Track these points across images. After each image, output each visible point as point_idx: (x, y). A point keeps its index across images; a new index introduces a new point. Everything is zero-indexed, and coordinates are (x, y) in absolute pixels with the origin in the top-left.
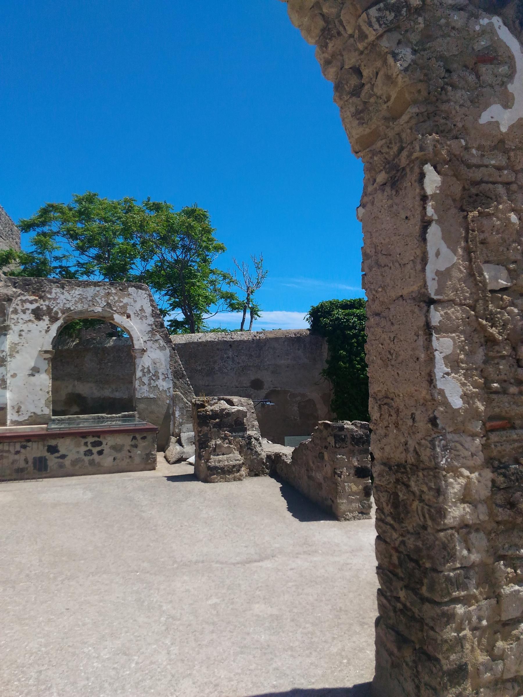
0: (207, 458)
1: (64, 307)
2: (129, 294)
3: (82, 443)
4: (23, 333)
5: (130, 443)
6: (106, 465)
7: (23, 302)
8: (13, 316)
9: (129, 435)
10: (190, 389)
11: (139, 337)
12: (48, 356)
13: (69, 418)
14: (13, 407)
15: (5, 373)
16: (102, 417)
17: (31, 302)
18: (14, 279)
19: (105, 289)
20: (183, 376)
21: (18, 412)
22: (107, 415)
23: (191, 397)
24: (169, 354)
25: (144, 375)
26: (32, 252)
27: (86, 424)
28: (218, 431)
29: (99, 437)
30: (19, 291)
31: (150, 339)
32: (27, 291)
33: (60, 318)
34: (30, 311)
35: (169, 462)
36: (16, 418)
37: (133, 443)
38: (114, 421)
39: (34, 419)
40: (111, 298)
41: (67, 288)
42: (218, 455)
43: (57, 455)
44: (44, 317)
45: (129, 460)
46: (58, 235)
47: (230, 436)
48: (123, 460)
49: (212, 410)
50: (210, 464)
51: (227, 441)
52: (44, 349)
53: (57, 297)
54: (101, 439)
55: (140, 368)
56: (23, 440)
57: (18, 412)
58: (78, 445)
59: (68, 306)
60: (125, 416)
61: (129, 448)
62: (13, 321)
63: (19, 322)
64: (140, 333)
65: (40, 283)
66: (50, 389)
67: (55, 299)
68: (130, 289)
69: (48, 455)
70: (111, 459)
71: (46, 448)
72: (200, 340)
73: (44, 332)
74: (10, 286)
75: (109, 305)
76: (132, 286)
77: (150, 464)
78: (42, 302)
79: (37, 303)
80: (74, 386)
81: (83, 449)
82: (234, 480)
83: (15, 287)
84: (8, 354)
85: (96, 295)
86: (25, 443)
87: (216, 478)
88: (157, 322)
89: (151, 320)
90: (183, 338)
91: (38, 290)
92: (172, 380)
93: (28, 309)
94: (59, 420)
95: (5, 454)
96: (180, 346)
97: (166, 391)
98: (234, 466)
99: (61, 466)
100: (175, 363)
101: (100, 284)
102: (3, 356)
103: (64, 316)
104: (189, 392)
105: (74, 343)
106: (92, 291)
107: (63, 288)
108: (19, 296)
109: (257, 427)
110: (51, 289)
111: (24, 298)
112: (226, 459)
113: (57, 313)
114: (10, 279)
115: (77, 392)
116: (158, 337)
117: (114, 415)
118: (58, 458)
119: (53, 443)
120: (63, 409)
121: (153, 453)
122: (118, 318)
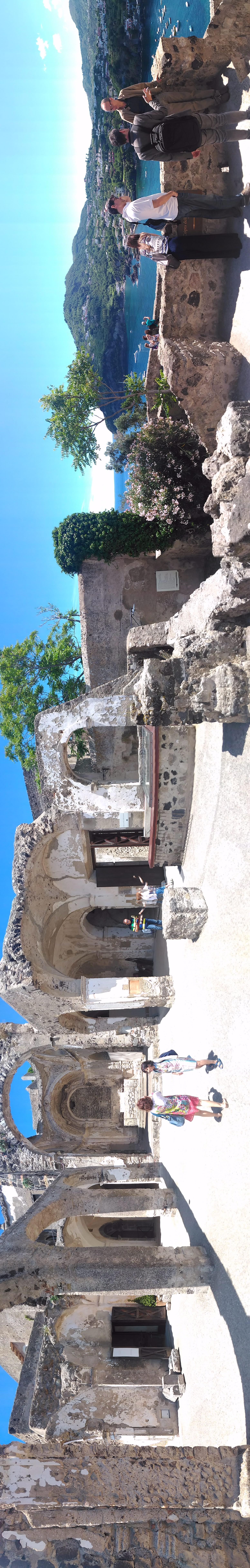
17: (60, 797)
30: (53, 805)
40: (48, 744)
41: (46, 776)
62: (73, 808)
65: (45, 792)
67: (55, 783)
75: (54, 747)
78: (58, 791)
85: (48, 756)
91: (50, 793)
93: (64, 799)
107: (46, 778)
109: (157, 625)
110: (48, 786)
111: (57, 802)
113: (64, 782)
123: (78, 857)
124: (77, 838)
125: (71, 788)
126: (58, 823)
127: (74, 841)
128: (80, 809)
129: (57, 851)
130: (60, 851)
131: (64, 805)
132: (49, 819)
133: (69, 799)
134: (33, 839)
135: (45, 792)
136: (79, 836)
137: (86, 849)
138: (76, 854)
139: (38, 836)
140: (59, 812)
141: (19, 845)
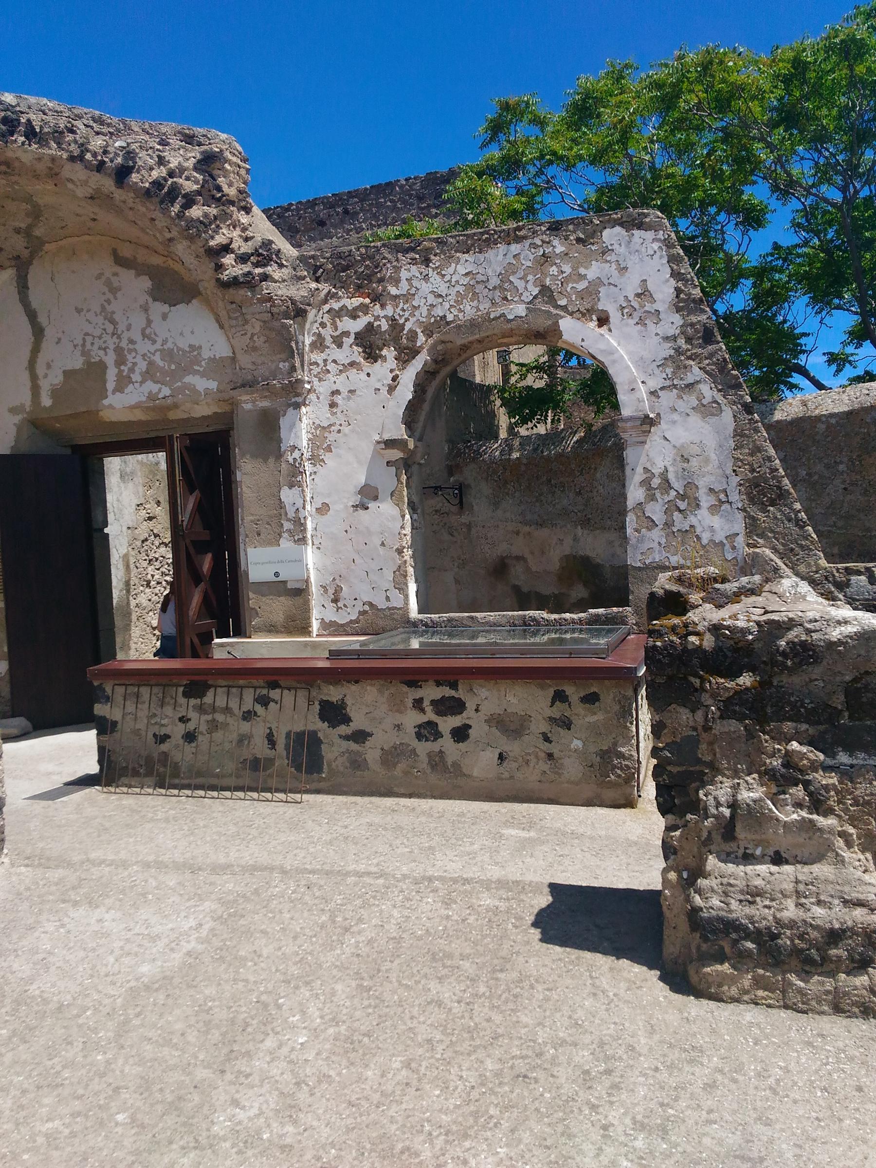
0: (691, 862)
1: (429, 315)
2: (605, 251)
3: (409, 702)
4: (338, 399)
6: (475, 774)
10: (807, 537)
13: (450, 620)
16: (534, 619)
17: (354, 317)
18: (313, 257)
19: (535, 246)
20: (781, 496)
23: (809, 565)
24: (731, 426)
25: (652, 498)
27: (493, 638)
28: (750, 735)
30: (325, 288)
31: (668, 383)
32: (344, 285)
33: (421, 347)
34: (351, 339)
36: (331, 615)
37: (557, 711)
38: (566, 632)
40: (554, 270)
41: (436, 261)
42: (747, 858)
44: (384, 352)
45: (544, 766)
46: (548, 193)
47: (815, 766)
48: (527, 762)
49: (716, 629)
50: (698, 900)
51: (798, 792)
52: (386, 436)
53: (413, 291)
54: (461, 693)
56: (261, 682)
59: (439, 312)
62: (316, 370)
63: (328, 371)
64: (637, 366)
65: (371, 258)
67: (408, 297)
68: (606, 233)
70: (491, 756)
71: (317, 707)
73: (384, 391)
74: (304, 278)
75: (546, 292)
77: (612, 785)
78: (377, 309)
79: (366, 314)
80: (576, 539)
82: (838, 1009)
83: (317, 280)
84: (307, 455)
85: (511, 269)
87: (733, 980)
88: (692, 325)
90: (845, 397)
91: (369, 278)
92: (744, 510)
93: (346, 334)
94: (426, 625)
96: (833, 421)
97: (722, 544)
98: (834, 936)
99: (357, 763)
101: (521, 233)
103: (431, 341)
104: (802, 547)
105: (575, 439)
106: (500, 257)
107: (427, 262)
108: (325, 302)
110: (397, 269)
111: (336, 306)
112: (789, 887)
113: (413, 335)
115: (581, 553)
116: (695, 373)
117: (567, 616)
118: (347, 738)
119: (333, 694)
120: (557, 592)
121: (622, 750)
123: (123, 383)
124: (202, 384)
125: (391, 363)
126: (257, 308)
127: (188, 370)
128: (312, 396)
129: (145, 298)
130: (145, 309)
131: (327, 333)
133: (351, 352)
134: (189, 201)
135: (371, 258)
136: (207, 392)
138: (137, 377)
139: (205, 224)
140: (300, 314)
141: (163, 143)
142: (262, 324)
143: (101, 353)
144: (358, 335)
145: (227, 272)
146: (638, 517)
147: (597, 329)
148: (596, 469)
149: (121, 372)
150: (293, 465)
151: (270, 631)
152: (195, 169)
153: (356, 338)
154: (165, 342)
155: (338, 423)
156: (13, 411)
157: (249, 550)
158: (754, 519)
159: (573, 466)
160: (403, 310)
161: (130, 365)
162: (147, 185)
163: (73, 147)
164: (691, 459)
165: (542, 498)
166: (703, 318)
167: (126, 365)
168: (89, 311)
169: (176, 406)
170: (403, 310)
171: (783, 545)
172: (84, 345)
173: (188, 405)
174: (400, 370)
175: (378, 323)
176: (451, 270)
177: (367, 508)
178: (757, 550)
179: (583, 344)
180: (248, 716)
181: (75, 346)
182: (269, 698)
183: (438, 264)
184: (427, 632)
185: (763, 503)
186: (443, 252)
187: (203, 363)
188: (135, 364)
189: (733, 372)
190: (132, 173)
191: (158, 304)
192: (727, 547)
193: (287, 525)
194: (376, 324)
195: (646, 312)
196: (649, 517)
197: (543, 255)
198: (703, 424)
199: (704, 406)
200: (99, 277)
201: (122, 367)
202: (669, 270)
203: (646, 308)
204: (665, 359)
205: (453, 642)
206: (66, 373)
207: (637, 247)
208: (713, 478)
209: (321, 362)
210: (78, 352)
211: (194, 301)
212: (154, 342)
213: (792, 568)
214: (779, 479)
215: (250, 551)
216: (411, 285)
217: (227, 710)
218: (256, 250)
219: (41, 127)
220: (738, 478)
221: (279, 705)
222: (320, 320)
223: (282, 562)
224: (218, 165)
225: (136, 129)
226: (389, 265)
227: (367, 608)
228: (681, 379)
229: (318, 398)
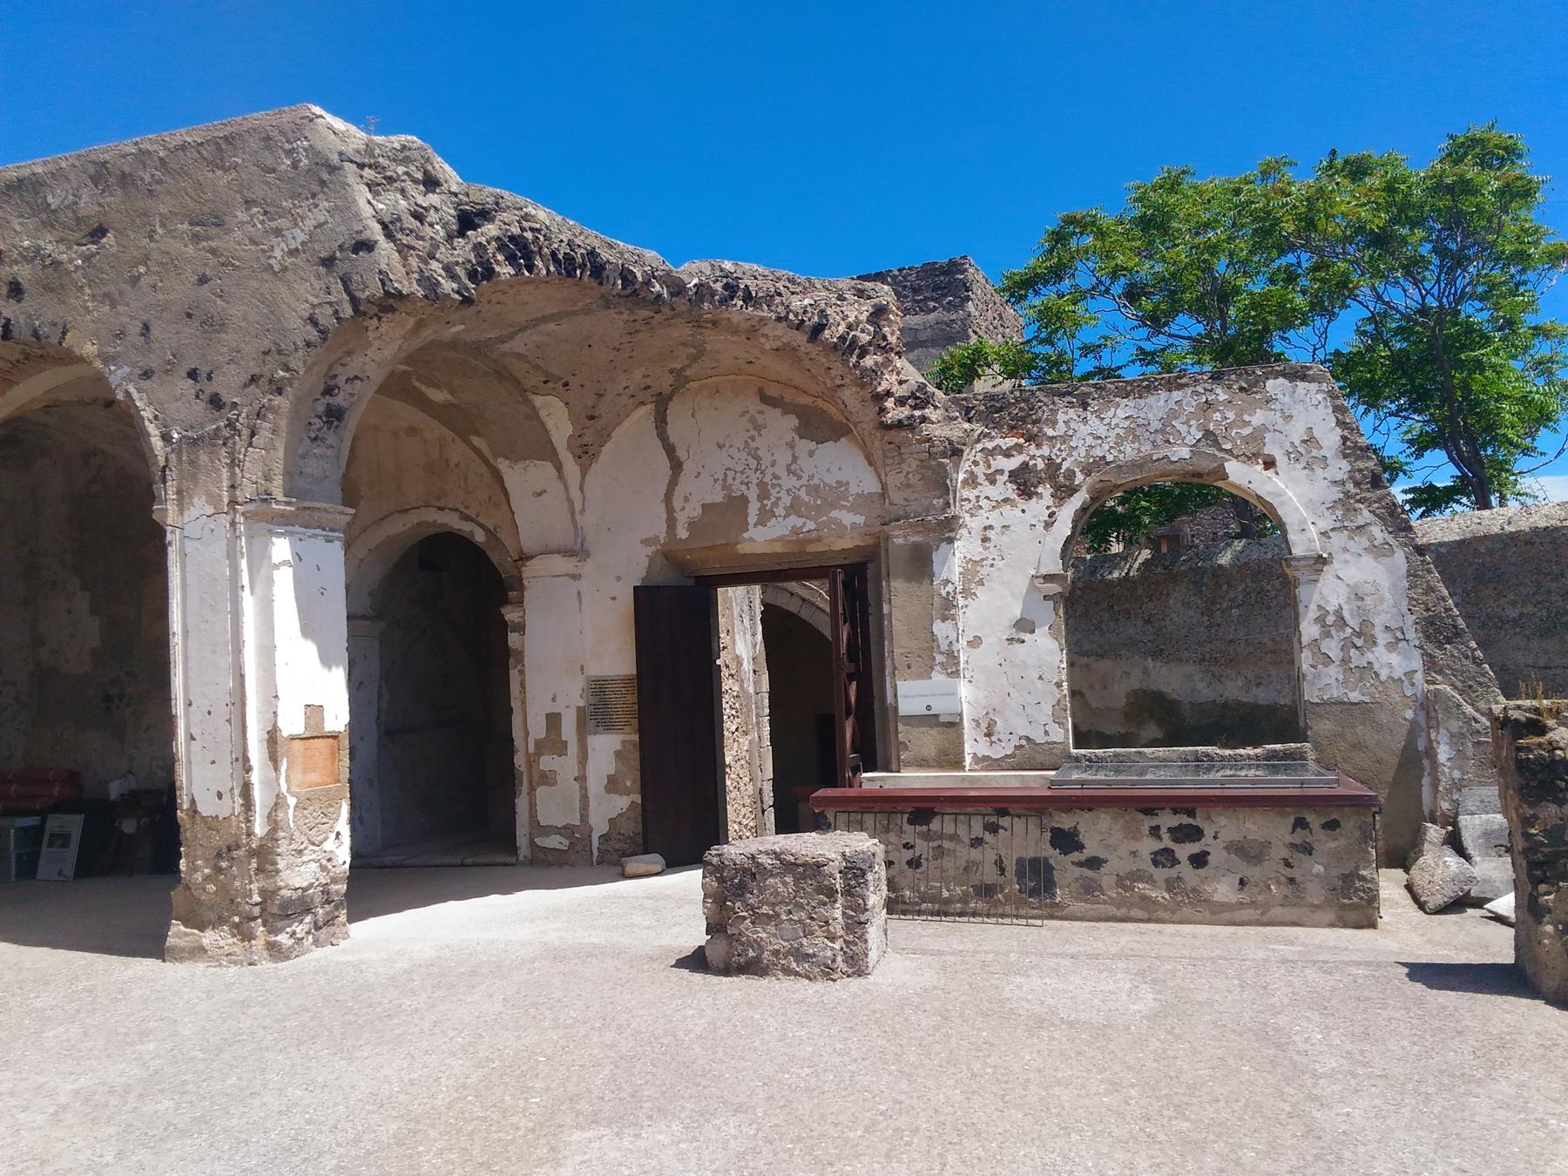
3: (1145, 829)
4: (991, 534)
5: (1289, 839)
7: (990, 453)
8: (966, 493)
9: (1282, 815)
10: (1484, 675)
11: (1305, 521)
12: (1054, 588)
13: (1116, 755)
14: (977, 722)
15: (953, 637)
16: (1207, 755)
17: (1007, 454)
18: (965, 399)
19: (1198, 394)
20: (1458, 633)
21: (989, 735)
22: (1218, 751)
25: (1327, 635)
26: (1029, 341)
29: (1192, 814)
30: (979, 428)
31: (1338, 525)
32: (997, 425)
34: (1006, 477)
35: (1421, 906)
36: (984, 749)
39: (1029, 756)
40: (1217, 416)
41: (1094, 405)
43: (1076, 856)
44: (1040, 490)
52: (1044, 571)
53: (1070, 433)
55: (1313, 613)
57: (989, 735)
58: (1134, 835)
59: (1098, 452)
60: (1274, 755)
61: (1285, 853)
62: (967, 506)
63: (981, 507)
64: (1307, 508)
66: (1064, 677)
67: (1065, 438)
68: (1270, 383)
69: (1053, 855)
72: (1509, 529)
73: (1040, 527)
76: (1277, 375)
78: (1033, 449)
79: (1021, 453)
80: (1145, 672)
81: (1148, 846)
83: (969, 421)
84: (959, 589)
85: (1173, 414)
86: (993, 819)
88: (1360, 471)
89: (1339, 469)
91: (1023, 419)
92: (1421, 648)
93: (1001, 472)
94: (1090, 760)
95: (947, 844)
100: (1426, 594)
101: (1183, 381)
102: (948, 593)
104: (1480, 684)
106: (1162, 403)
107: (1085, 406)
108: (978, 441)
110: (1054, 412)
111: (990, 445)
113: (1070, 474)
114: (955, 401)
116: (1365, 516)
117: (1241, 751)
120: (1123, 731)
122: (1241, 475)
123: (765, 516)
124: (848, 518)
125: (1048, 500)
127: (833, 505)
129: (790, 435)
130: (791, 445)
131: (980, 471)
132: (928, 412)
135: (1026, 401)
136: (854, 526)
137: (795, 549)
138: (780, 511)
140: (956, 453)
141: (841, 298)
142: (919, 463)
143: (744, 487)
144: (1012, 473)
145: (890, 415)
146: (1313, 653)
147: (1264, 472)
148: (1168, 595)
149: (762, 510)
150: (947, 599)
151: (920, 766)
152: (868, 321)
153: (1010, 476)
154: (811, 477)
155: (991, 557)
156: (646, 542)
157: (898, 683)
158: (1430, 655)
159: (1140, 592)
160: (1060, 450)
161: (773, 500)
162: (835, 340)
163: (780, 309)
164: (1365, 597)
165: (1103, 626)
166: (1371, 464)
167: (769, 499)
168: (731, 446)
169: (819, 540)
170: (1060, 450)
171: (1463, 682)
172: (725, 480)
173: (832, 539)
174: (1056, 507)
175: (1034, 462)
176: (1111, 414)
177: (1023, 642)
178: (1437, 686)
179: (1250, 486)
180: (977, 842)
181: (715, 481)
182: (998, 825)
183: (1096, 408)
184: (1091, 767)
185: (1440, 642)
186: (1100, 396)
187: (850, 498)
188: (779, 499)
189: (1403, 516)
190: (824, 329)
191: (804, 441)
192: (1406, 683)
193: (939, 658)
194: (1031, 463)
195: (1313, 457)
196: (1325, 654)
197: (1206, 402)
198: (1376, 565)
199: (1375, 547)
200: (743, 414)
201: (765, 502)
202: (1334, 420)
203: (1313, 454)
204: (1335, 502)
205: (1119, 778)
206: (706, 507)
207: (1302, 397)
208: (1388, 617)
209: (973, 498)
210: (718, 486)
211: (842, 439)
212: (800, 478)
213: (1472, 705)
214: (1453, 618)
215: (902, 686)
216: (1069, 427)
217: (954, 837)
218: (913, 393)
219: (757, 292)
220: (1414, 617)
221: (1009, 833)
222: (972, 459)
223: (935, 695)
224: (885, 317)
225: (819, 286)
226: (1045, 408)
227: (1024, 742)
228: (1352, 521)
229: (970, 533)
